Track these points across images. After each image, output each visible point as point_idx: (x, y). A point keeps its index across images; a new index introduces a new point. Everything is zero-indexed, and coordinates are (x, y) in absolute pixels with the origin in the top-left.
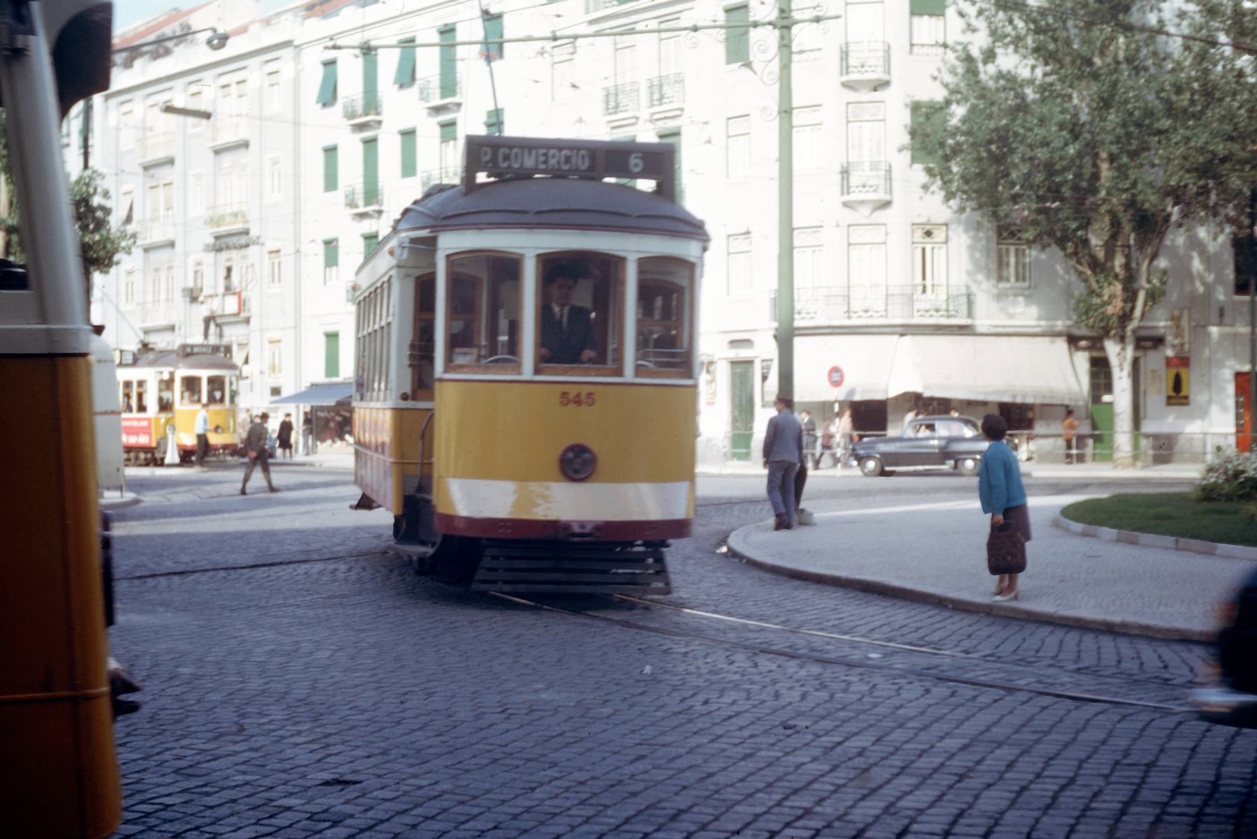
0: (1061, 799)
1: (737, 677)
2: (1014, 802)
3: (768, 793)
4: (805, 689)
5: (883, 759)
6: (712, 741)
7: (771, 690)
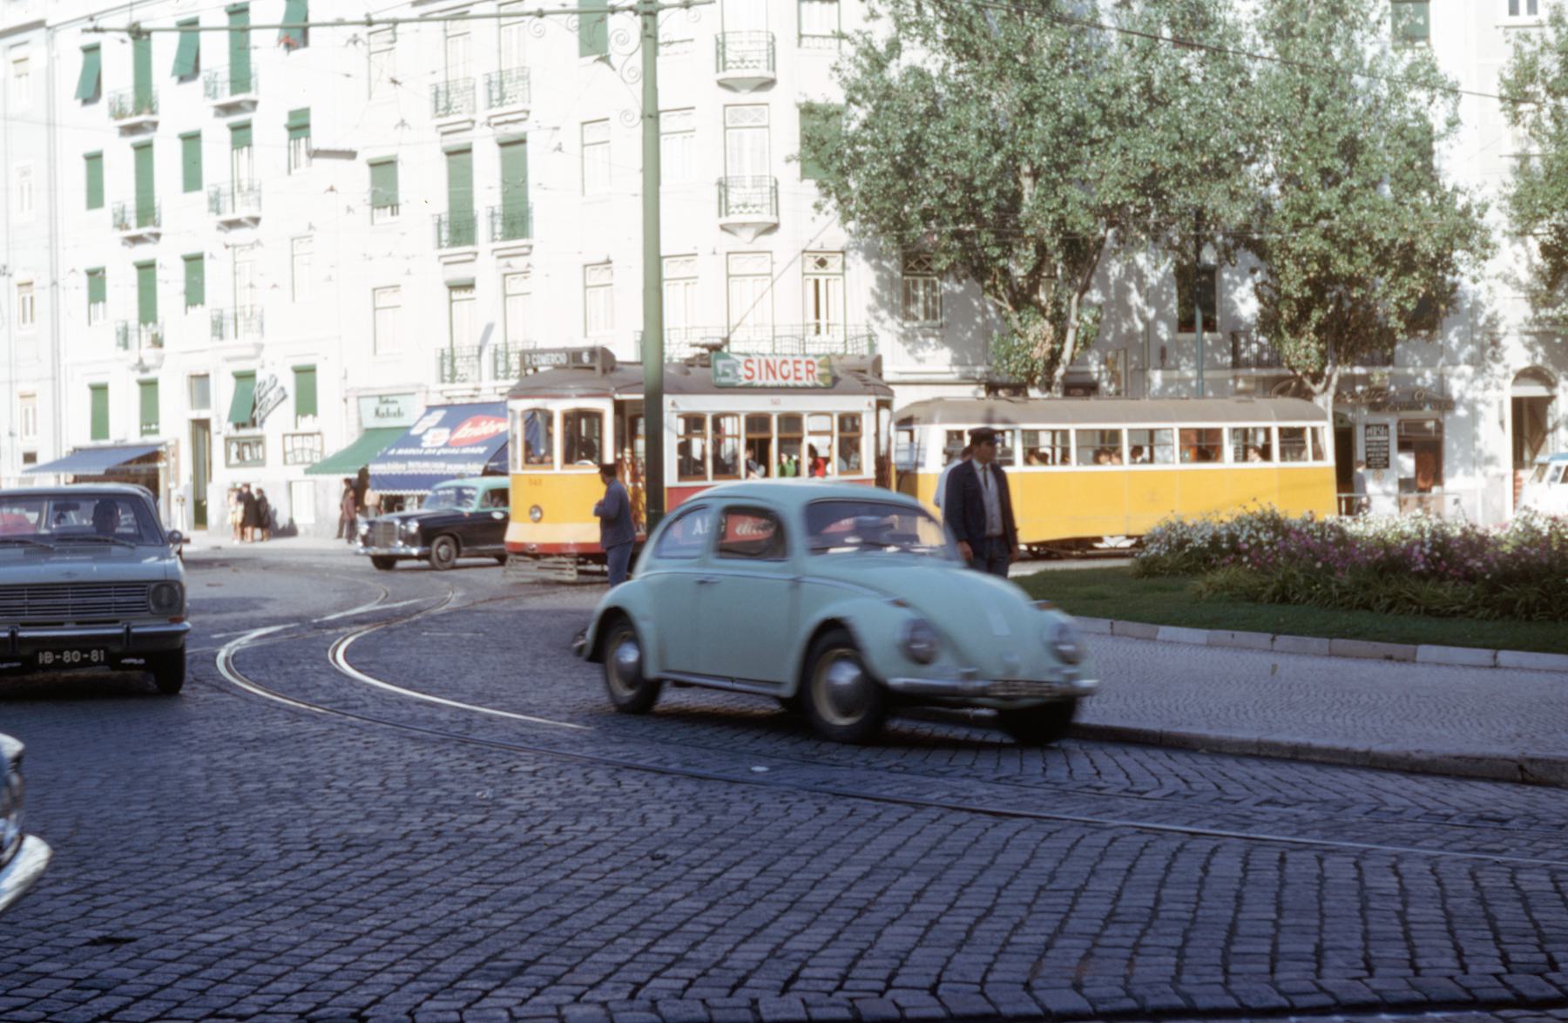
0: (976, 933)
1: (597, 799)
2: (922, 938)
3: (633, 938)
4: (676, 811)
5: (768, 892)
6: (567, 877)
7: (636, 813)
